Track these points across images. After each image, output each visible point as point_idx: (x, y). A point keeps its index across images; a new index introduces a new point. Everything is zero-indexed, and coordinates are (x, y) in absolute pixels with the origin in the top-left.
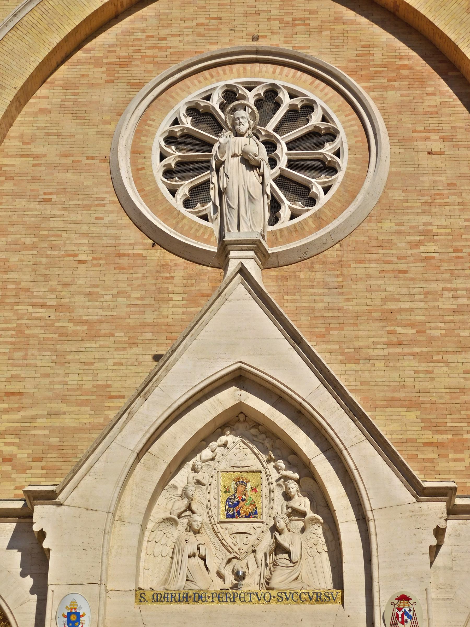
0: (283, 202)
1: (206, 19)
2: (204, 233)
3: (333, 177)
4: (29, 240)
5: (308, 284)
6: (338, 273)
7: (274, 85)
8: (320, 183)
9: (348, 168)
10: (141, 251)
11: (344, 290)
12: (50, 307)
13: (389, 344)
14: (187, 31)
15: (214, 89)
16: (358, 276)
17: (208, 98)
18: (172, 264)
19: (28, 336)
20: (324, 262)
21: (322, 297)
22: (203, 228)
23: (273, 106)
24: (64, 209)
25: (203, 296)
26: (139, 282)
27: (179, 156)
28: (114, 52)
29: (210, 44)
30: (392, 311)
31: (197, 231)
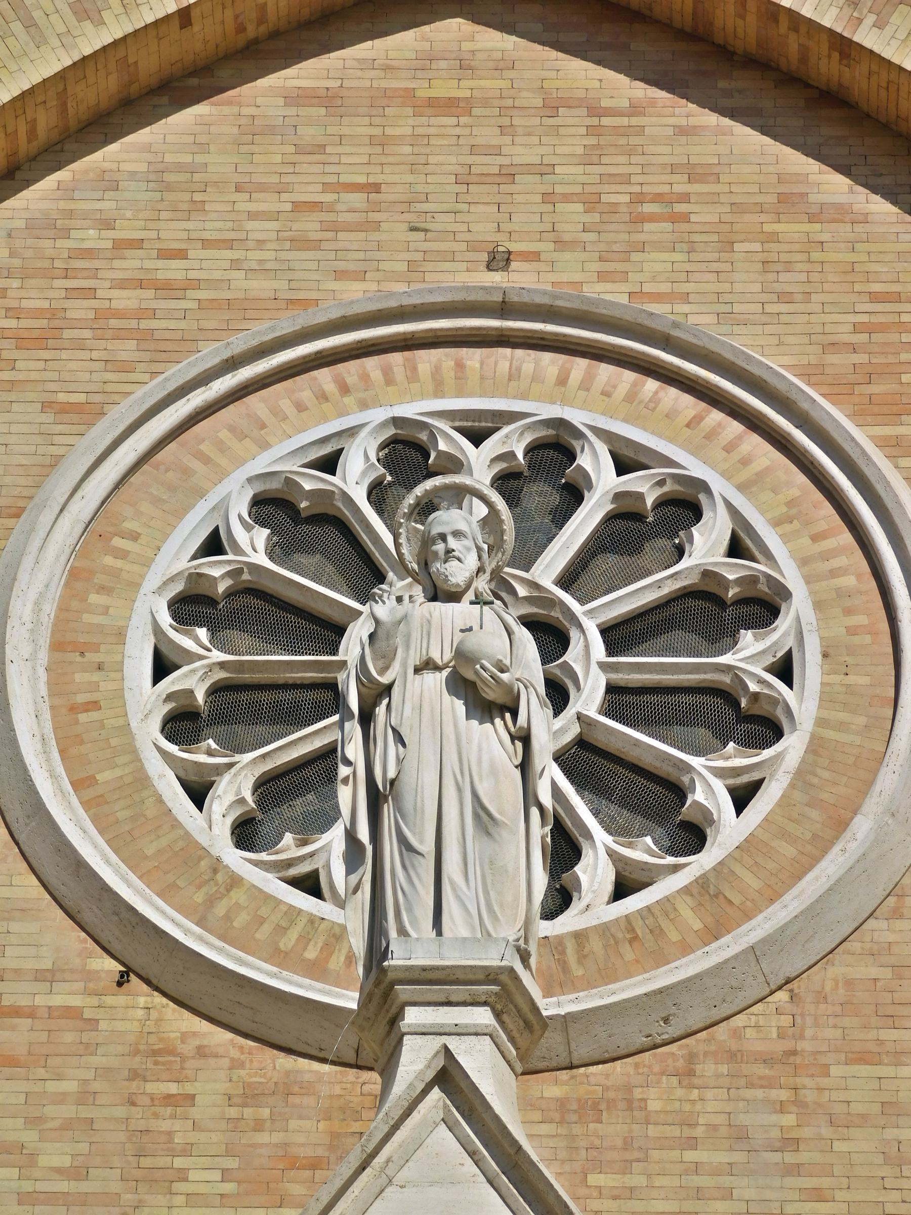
0: (589, 836)
1: (327, 187)
2: (304, 940)
3: (767, 753)
5: (675, 1131)
6: (784, 1095)
7: (560, 423)
8: (720, 773)
9: (821, 722)
10: (75, 1001)
11: (804, 1157)
15: (352, 432)
16: (856, 1108)
17: (329, 464)
18: (188, 1048)
20: (733, 1056)
21: (726, 1181)
22: (302, 923)
23: (555, 498)
25: (292, 1167)
26: (68, 1111)
27: (222, 665)
29: (339, 275)
31: (281, 930)
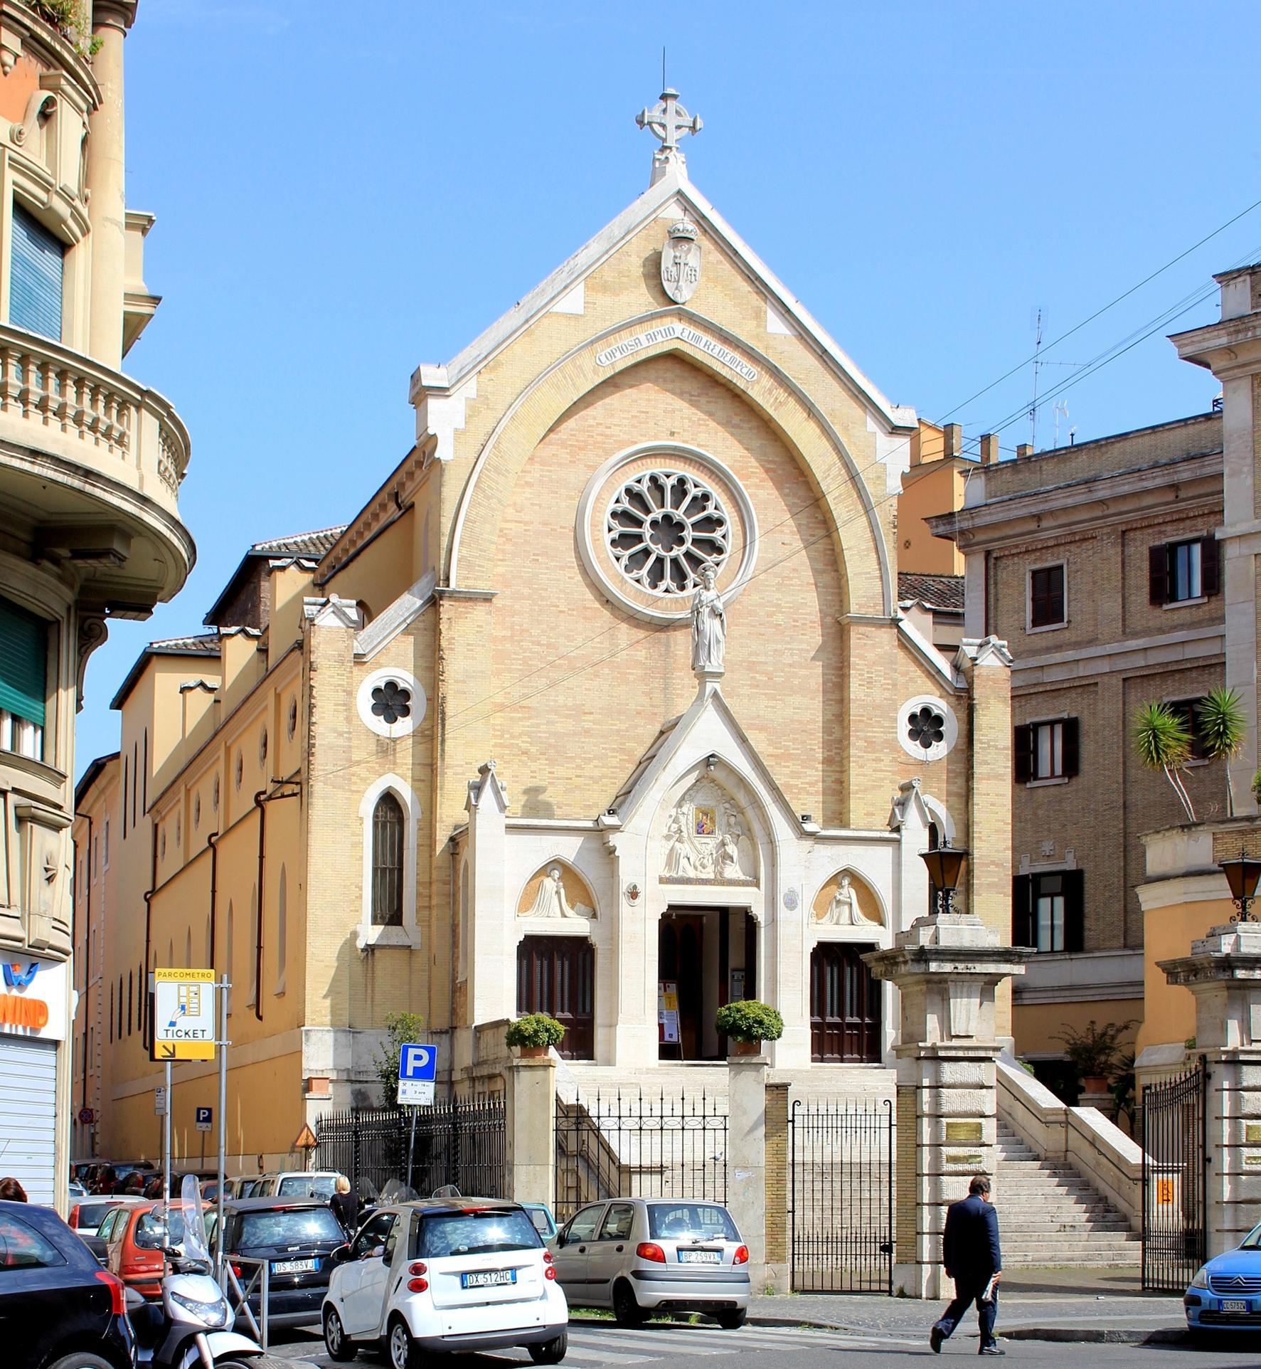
4: (526, 591)
12: (543, 645)
13: (752, 686)
14: (626, 422)
19: (531, 665)
24: (547, 568)
28: (575, 435)
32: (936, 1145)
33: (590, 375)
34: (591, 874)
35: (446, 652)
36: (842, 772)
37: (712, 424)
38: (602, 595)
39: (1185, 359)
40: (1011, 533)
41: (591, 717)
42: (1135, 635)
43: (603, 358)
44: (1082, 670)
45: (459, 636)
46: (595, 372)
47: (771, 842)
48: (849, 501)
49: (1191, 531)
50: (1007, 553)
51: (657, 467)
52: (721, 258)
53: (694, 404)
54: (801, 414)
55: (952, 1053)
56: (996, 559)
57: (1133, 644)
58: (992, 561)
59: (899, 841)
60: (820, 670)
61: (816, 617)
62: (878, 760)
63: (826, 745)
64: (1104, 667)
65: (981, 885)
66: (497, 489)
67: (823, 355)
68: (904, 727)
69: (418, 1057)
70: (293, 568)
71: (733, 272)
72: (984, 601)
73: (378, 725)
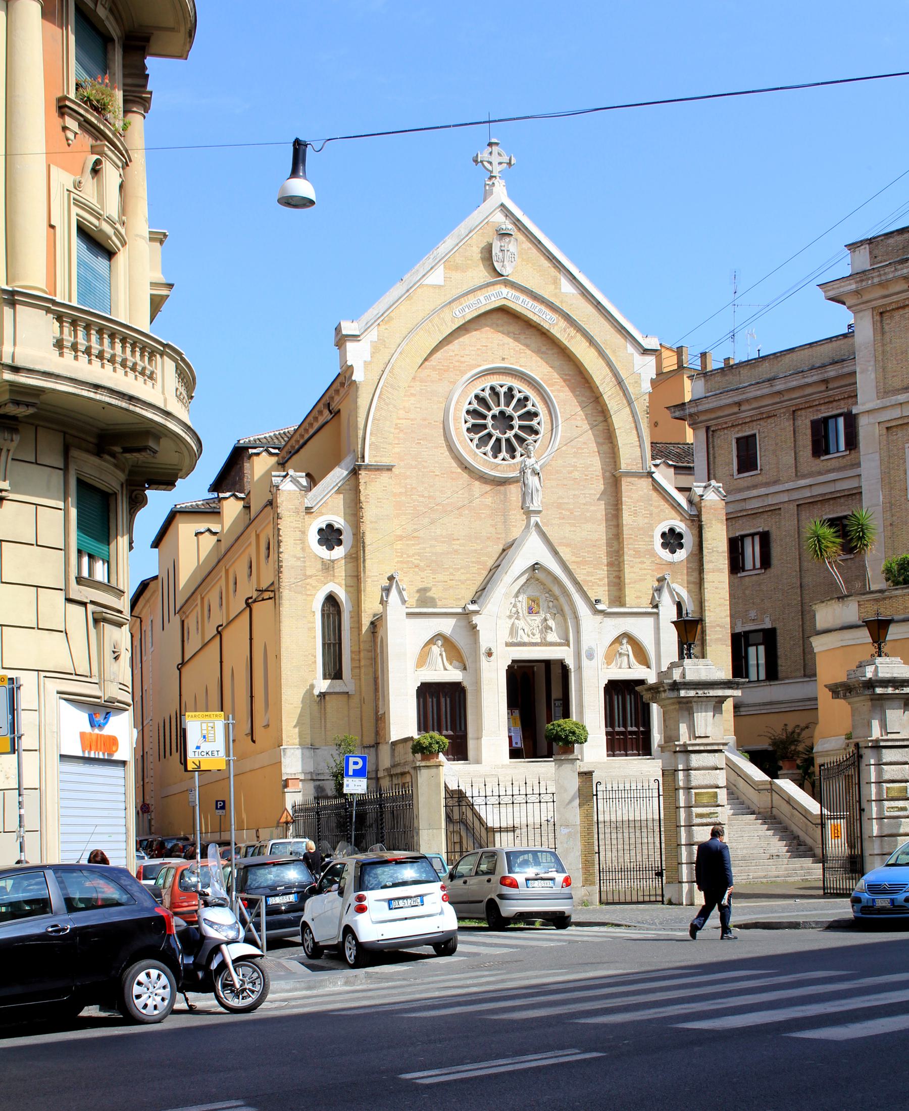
4: (414, 463)
13: (560, 518)
14: (473, 353)
30: (561, 503)
32: (689, 807)
33: (449, 324)
34: (462, 642)
35: (364, 504)
36: (620, 571)
37: (529, 352)
38: (462, 464)
39: (829, 299)
40: (722, 414)
41: (458, 542)
42: (804, 477)
43: (457, 313)
44: (771, 500)
45: (372, 493)
46: (453, 322)
47: (576, 618)
48: (618, 398)
49: (837, 409)
50: (720, 427)
51: (495, 381)
52: (530, 245)
53: (516, 339)
54: (585, 344)
55: (697, 748)
56: (713, 431)
57: (803, 482)
58: (711, 433)
59: (657, 614)
60: (603, 507)
61: (599, 472)
62: (644, 563)
63: (609, 554)
64: (785, 498)
65: (711, 640)
66: (393, 399)
67: (598, 305)
68: (658, 541)
69: (356, 763)
70: (264, 454)
71: (538, 254)
72: (706, 458)
73: (323, 552)
